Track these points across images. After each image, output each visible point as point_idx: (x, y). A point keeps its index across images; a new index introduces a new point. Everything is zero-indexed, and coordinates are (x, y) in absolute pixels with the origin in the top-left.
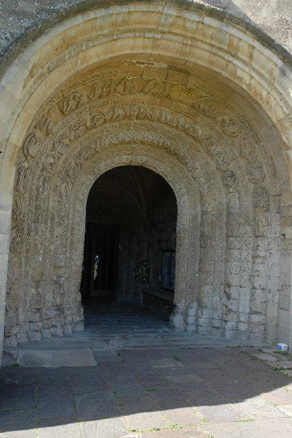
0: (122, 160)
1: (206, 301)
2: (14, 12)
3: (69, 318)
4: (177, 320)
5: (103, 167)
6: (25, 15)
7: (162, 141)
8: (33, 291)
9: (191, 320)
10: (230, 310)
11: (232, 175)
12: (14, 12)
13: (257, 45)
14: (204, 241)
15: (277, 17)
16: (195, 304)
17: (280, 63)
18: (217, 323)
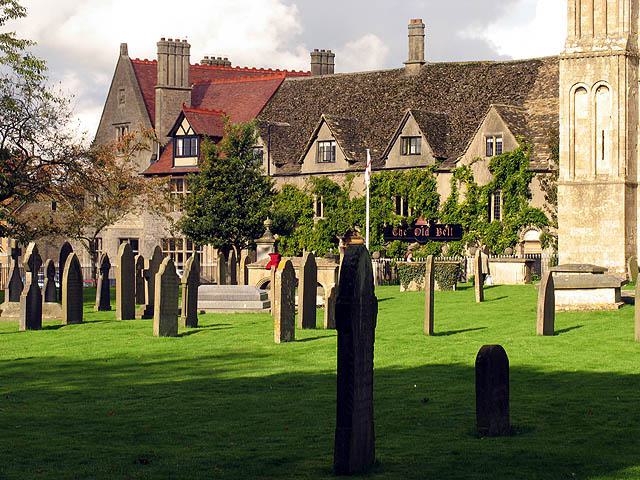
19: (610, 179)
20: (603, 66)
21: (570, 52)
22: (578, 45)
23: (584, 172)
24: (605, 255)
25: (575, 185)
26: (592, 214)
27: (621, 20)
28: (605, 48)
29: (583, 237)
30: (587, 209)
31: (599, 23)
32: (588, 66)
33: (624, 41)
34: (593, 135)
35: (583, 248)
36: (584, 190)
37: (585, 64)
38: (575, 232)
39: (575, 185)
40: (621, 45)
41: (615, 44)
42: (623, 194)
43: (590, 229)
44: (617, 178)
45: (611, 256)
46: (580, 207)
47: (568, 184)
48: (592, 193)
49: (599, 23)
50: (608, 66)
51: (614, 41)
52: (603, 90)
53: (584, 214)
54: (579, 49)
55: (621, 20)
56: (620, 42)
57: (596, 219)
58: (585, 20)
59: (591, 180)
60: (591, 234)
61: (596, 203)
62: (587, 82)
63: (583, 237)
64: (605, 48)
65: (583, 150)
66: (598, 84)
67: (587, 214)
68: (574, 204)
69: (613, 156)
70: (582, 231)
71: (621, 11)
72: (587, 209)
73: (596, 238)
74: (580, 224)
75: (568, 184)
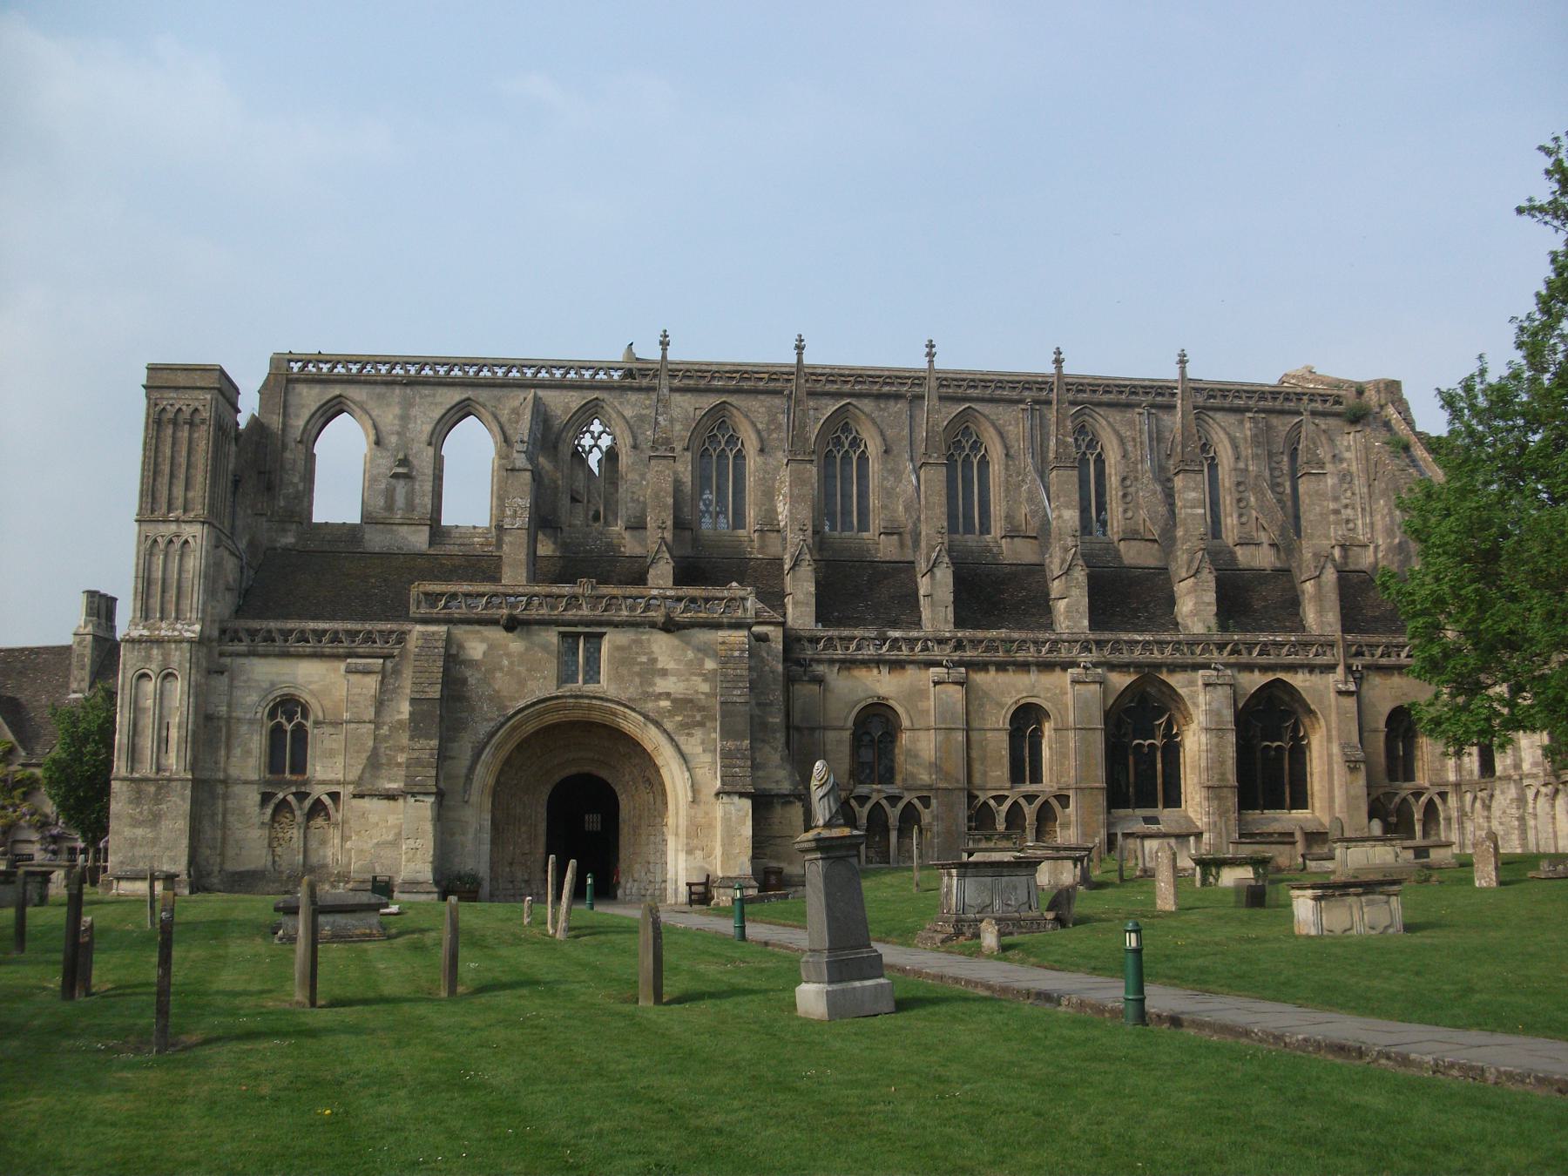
0: (573, 770)
1: (636, 876)
2: (486, 720)
3: (535, 891)
4: (620, 892)
5: (557, 778)
6: (492, 719)
7: (596, 757)
8: (508, 869)
9: (628, 892)
10: (650, 881)
11: (648, 780)
12: (486, 720)
13: (626, 710)
14: (636, 828)
15: (640, 691)
16: (630, 880)
17: (643, 719)
18: (643, 892)
21: (135, 634)
22: (144, 627)
25: (133, 780)
26: (150, 811)
27: (195, 606)
28: (176, 633)
29: (139, 838)
30: (145, 807)
32: (155, 651)
35: (139, 852)
37: (152, 648)
38: (128, 832)
40: (193, 632)
41: (187, 631)
42: (188, 792)
43: (149, 830)
44: (182, 775)
45: (173, 860)
47: (124, 779)
48: (152, 789)
50: (178, 653)
51: (186, 627)
52: (170, 679)
53: (141, 813)
54: (145, 632)
55: (195, 606)
57: (155, 820)
59: (152, 776)
60: (150, 835)
61: (157, 799)
65: (147, 743)
67: (145, 813)
70: (140, 832)
71: (195, 596)
73: (154, 842)
74: (136, 823)
75: (124, 779)
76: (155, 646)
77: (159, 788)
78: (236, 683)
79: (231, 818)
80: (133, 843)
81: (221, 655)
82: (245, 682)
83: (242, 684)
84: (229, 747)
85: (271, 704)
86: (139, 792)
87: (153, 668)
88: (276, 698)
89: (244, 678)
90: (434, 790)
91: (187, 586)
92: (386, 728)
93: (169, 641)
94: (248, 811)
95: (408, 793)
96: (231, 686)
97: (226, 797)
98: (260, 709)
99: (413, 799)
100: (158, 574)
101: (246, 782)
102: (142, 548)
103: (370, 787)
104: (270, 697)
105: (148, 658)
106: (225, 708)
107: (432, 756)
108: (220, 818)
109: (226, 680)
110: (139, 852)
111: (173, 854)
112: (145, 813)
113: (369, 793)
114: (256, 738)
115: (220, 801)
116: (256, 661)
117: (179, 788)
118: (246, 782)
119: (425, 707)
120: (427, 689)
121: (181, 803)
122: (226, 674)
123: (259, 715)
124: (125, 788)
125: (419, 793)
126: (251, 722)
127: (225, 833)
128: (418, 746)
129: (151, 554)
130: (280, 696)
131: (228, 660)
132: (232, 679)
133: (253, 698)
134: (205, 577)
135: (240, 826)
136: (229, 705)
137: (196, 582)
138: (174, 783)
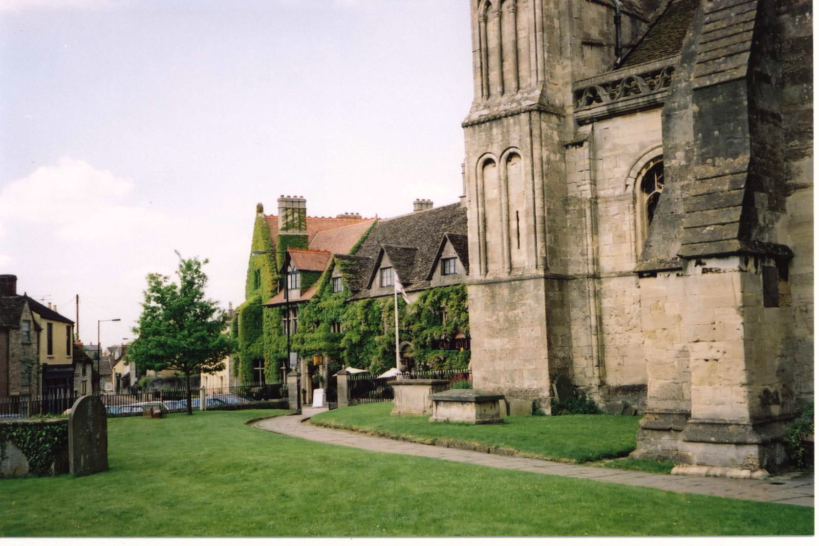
19: (527, 274)
20: (511, 129)
23: (498, 269)
24: (526, 374)
25: (487, 283)
26: (507, 319)
27: (533, 68)
29: (498, 350)
30: (501, 314)
31: (510, 77)
33: (538, 92)
34: (504, 218)
36: (497, 288)
37: (491, 128)
39: (487, 283)
41: (527, 99)
42: (542, 293)
43: (506, 340)
44: (534, 272)
46: (493, 311)
47: (480, 283)
49: (510, 77)
50: (517, 128)
52: (514, 160)
53: (498, 321)
54: (486, 112)
56: (532, 95)
57: (511, 326)
58: (494, 76)
59: (504, 276)
61: (512, 306)
62: (495, 152)
63: (498, 350)
64: (514, 105)
65: (495, 239)
66: (507, 153)
67: (501, 320)
68: (486, 308)
69: (528, 244)
70: (498, 343)
72: (501, 314)
73: (512, 353)
74: (495, 333)
75: (480, 283)
76: (494, 124)
77: (513, 290)
78: (600, 154)
79: (606, 320)
80: (493, 356)
81: (581, 122)
82: (611, 150)
83: (607, 154)
84: (595, 230)
85: (644, 172)
86: (493, 297)
87: (495, 152)
88: (647, 164)
89: (608, 146)
90: (736, 245)
91: (522, 45)
92: (680, 154)
93: (506, 116)
94: (627, 311)
95: (689, 259)
96: (594, 158)
97: (597, 295)
98: (631, 181)
99: (699, 269)
100: (493, 43)
101: (622, 275)
102: (476, 16)
103: (663, 257)
104: (641, 164)
105: (490, 141)
106: (588, 187)
107: (734, 185)
108: (593, 321)
109: (587, 151)
110: (500, 365)
111: (533, 367)
112: (501, 320)
113: (662, 267)
114: (629, 217)
115: (592, 300)
116: (618, 121)
117: (532, 287)
118: (622, 275)
119: (720, 99)
120: (723, 67)
121: (536, 305)
122: (586, 144)
123: (630, 189)
124: (480, 294)
125: (709, 257)
126: (619, 199)
127: (602, 339)
128: (712, 171)
129: (486, 20)
130: (653, 160)
131: (586, 129)
132: (594, 150)
133: (623, 168)
134: (543, 30)
135: (619, 329)
136: (594, 182)
137: (532, 38)
138: (527, 283)
